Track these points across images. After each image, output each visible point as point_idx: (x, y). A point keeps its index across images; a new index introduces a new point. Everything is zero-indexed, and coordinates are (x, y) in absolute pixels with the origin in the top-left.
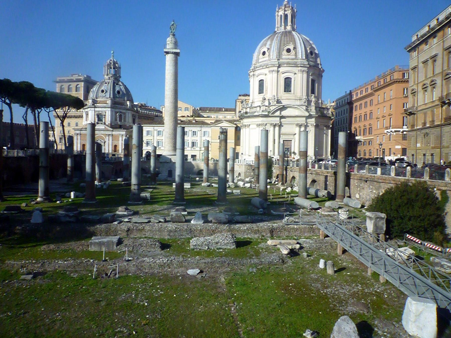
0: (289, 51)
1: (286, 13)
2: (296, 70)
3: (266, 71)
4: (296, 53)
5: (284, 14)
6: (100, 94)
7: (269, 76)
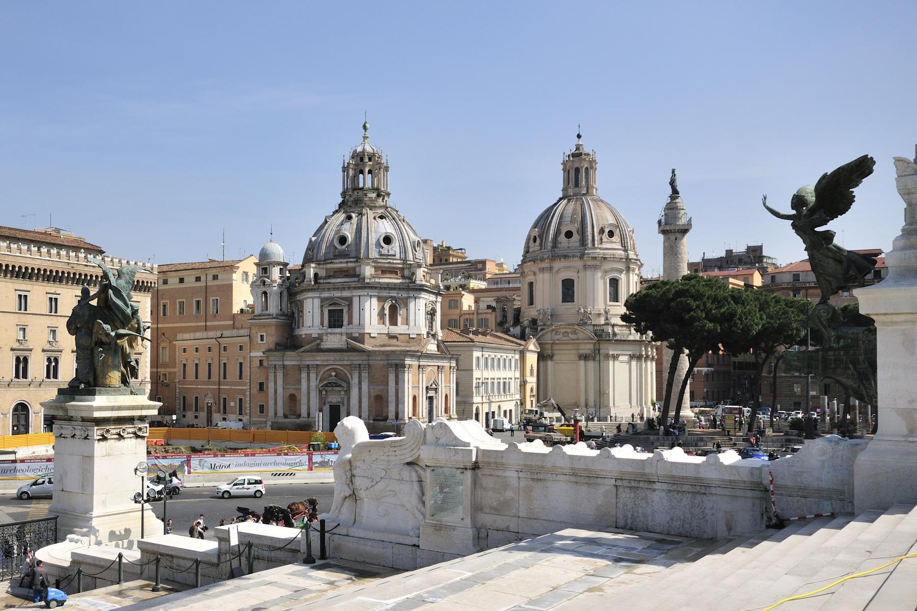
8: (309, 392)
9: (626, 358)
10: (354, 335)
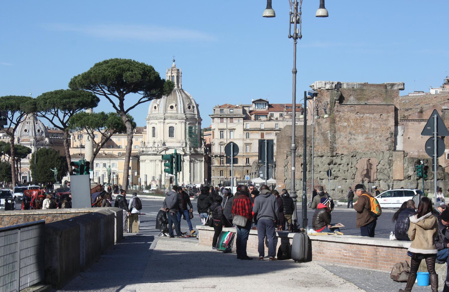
0: (172, 107)
3: (156, 121)
4: (177, 109)
6: (24, 133)
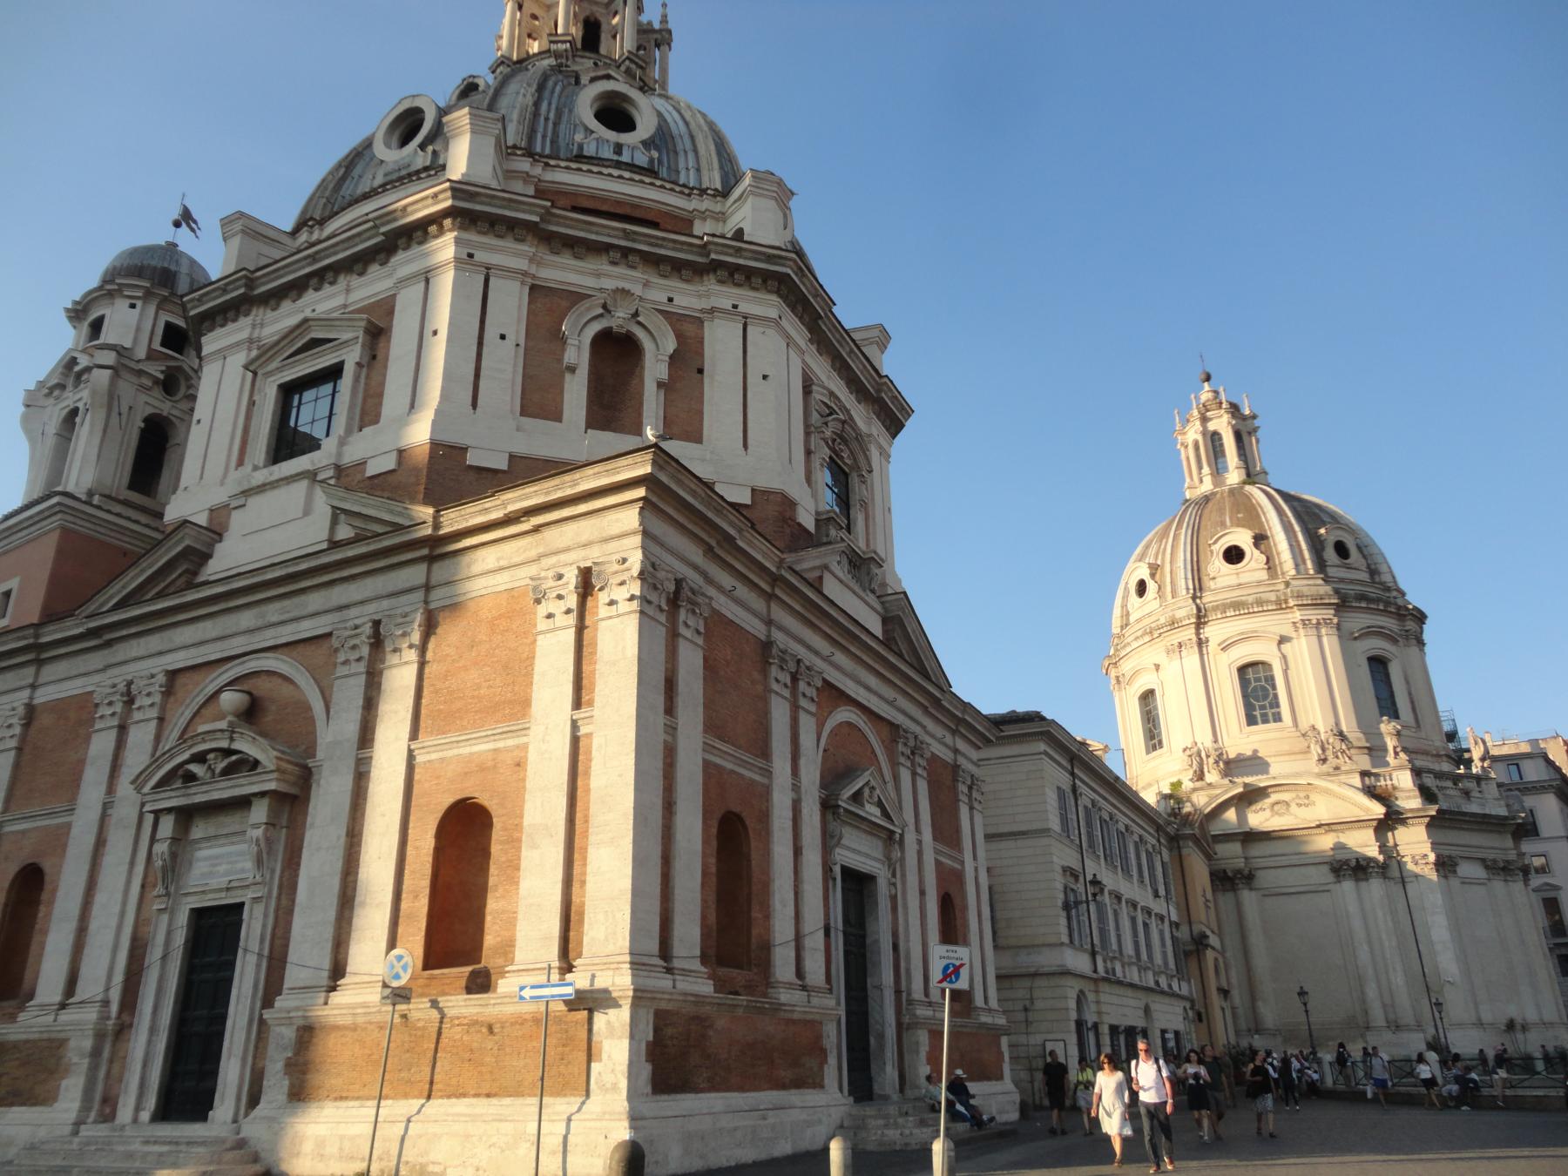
0: (1234, 555)
1: (1212, 426)
2: (1279, 623)
3: (1154, 653)
5: (1204, 433)
7: (1171, 667)
8: (100, 843)
9: (1477, 871)
10: (371, 470)
